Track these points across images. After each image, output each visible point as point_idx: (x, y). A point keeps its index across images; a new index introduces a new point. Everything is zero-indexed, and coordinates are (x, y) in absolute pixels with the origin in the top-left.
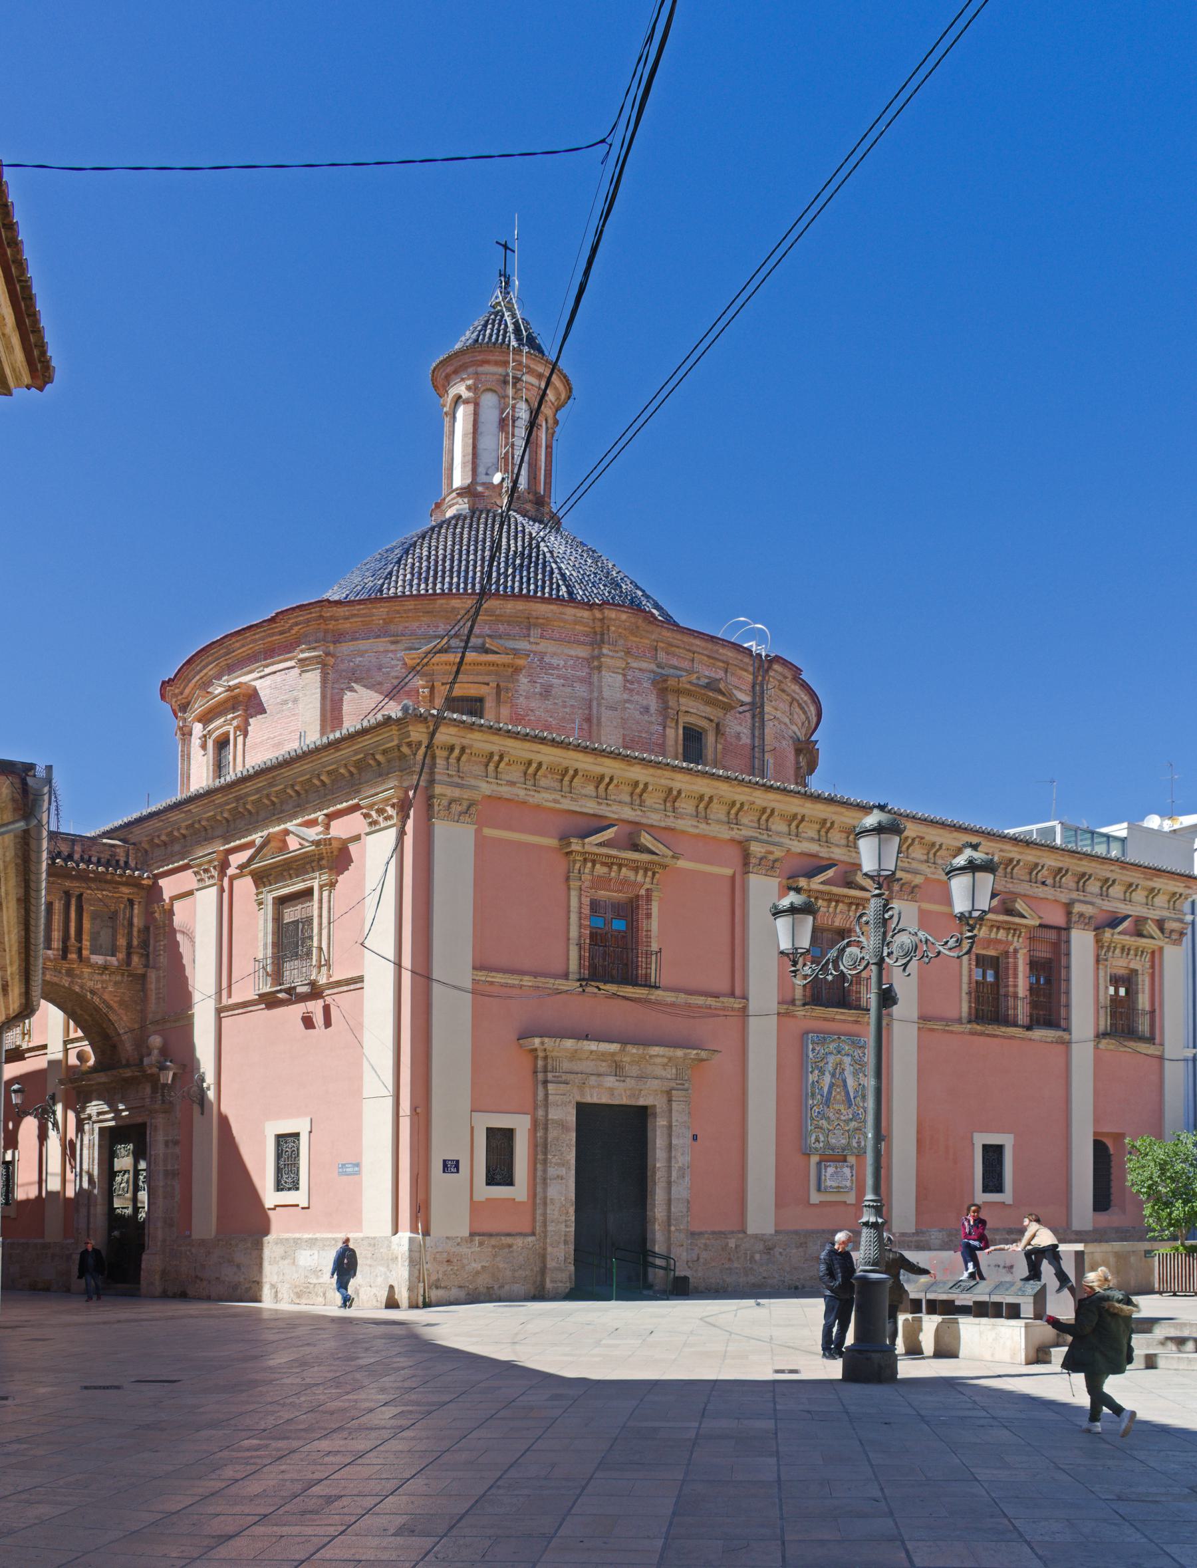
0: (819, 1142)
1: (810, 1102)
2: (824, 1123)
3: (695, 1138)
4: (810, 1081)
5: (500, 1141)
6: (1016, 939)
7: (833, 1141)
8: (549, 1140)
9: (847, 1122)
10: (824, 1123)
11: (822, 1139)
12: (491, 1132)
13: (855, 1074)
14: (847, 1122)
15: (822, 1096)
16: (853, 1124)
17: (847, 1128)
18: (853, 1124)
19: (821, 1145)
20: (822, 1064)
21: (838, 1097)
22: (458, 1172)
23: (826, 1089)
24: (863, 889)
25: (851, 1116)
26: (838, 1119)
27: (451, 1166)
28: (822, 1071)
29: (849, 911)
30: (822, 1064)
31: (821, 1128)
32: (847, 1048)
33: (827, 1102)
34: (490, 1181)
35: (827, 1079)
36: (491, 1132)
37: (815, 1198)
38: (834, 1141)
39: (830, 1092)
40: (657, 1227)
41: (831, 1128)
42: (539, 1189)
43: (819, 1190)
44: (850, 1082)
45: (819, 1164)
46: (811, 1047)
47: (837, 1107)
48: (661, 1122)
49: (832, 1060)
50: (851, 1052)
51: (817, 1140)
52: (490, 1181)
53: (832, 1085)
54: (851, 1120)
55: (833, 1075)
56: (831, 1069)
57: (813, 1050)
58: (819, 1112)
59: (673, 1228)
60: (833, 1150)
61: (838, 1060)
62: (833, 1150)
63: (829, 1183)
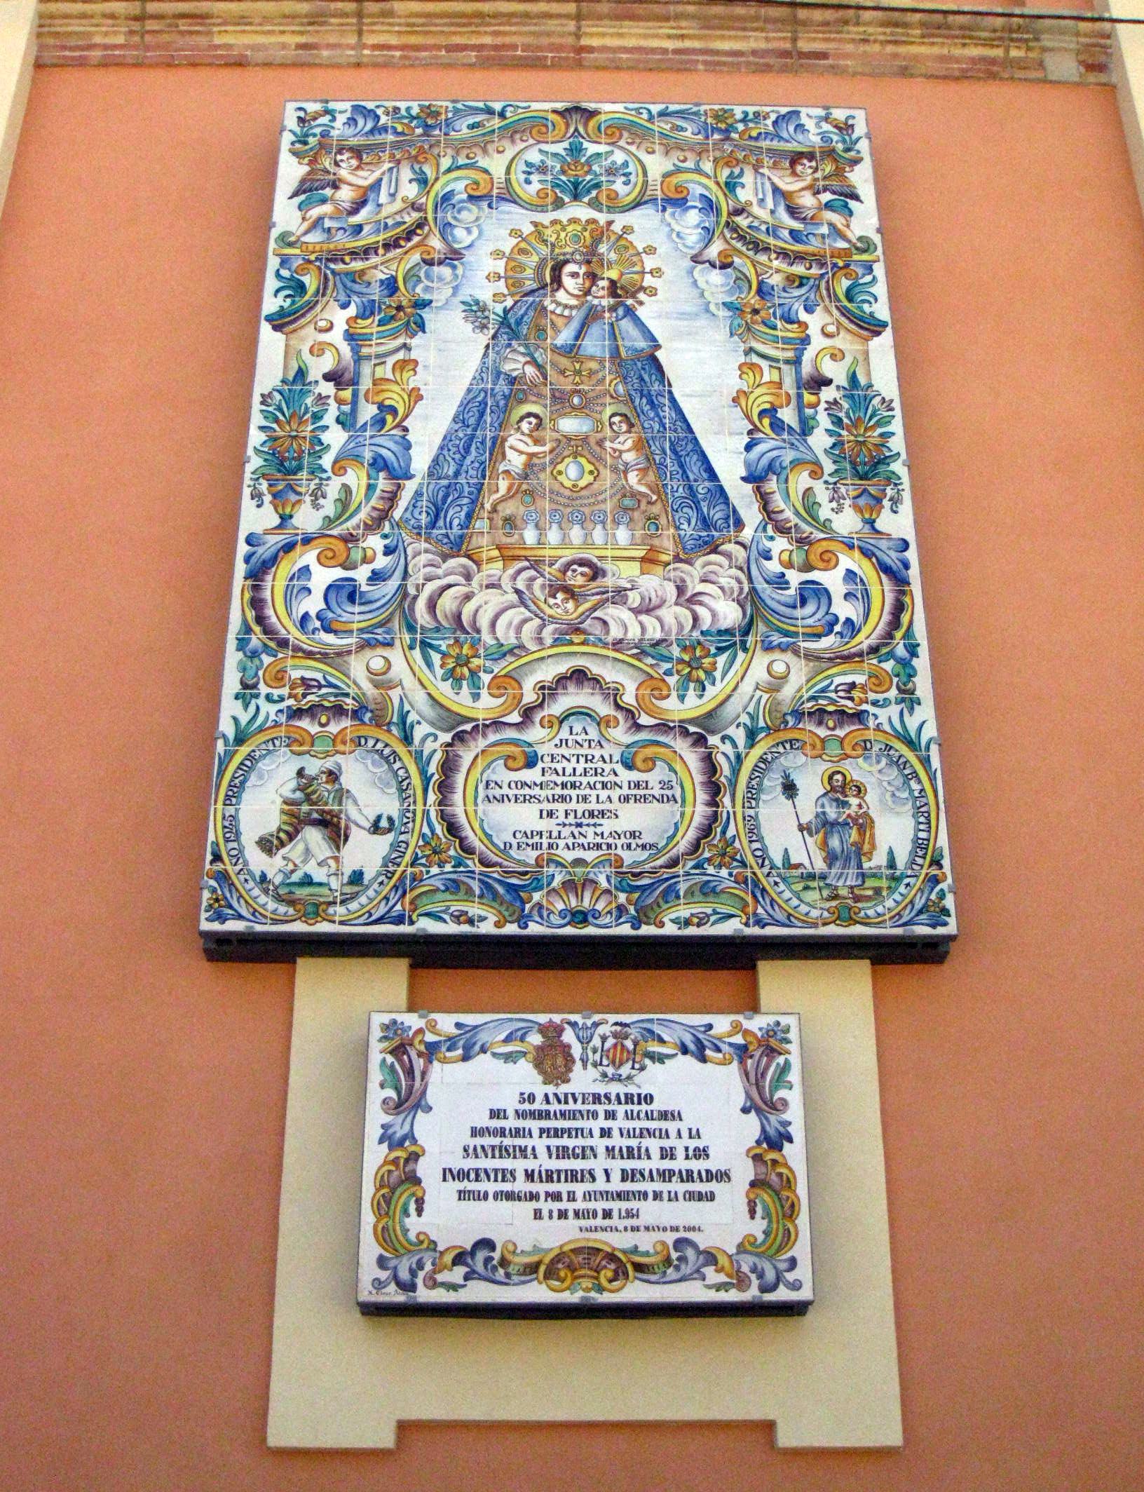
0: (335, 829)
17: (689, 706)
20: (379, 269)
21: (571, 471)
25: (730, 614)
32: (657, 165)
38: (525, 817)
41: (487, 705)
46: (290, 171)
57: (307, 189)
58: (346, 592)
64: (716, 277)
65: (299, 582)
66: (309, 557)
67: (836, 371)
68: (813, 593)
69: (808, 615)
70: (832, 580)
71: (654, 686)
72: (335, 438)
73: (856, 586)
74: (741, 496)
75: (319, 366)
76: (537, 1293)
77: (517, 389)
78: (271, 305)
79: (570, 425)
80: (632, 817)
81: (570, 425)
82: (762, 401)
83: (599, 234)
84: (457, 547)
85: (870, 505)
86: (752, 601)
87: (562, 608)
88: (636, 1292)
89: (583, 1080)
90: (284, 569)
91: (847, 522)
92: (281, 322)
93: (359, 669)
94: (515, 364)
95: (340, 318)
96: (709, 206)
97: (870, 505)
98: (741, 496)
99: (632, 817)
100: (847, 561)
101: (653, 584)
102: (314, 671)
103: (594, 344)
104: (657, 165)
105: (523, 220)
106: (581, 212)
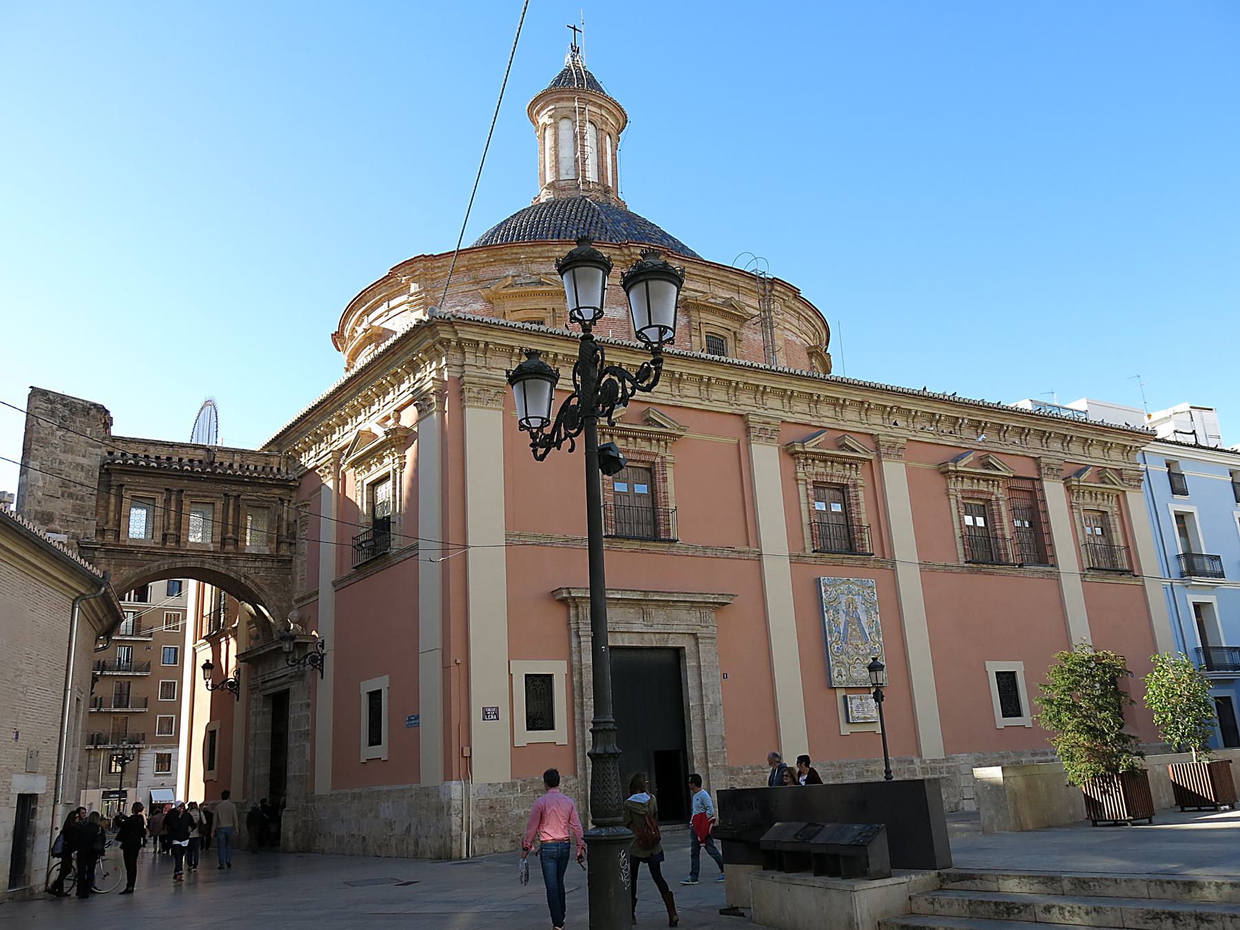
1: (829, 639)
3: (725, 676)
5: (539, 687)
6: (996, 488)
8: (584, 685)
11: (844, 673)
13: (867, 611)
21: (854, 633)
22: (498, 719)
23: (842, 627)
24: (854, 450)
26: (857, 653)
27: (490, 714)
29: (844, 470)
31: (843, 663)
32: (857, 589)
33: (845, 639)
34: (531, 726)
37: (846, 730)
39: (846, 629)
40: (695, 764)
42: (578, 732)
43: (848, 722)
45: (845, 698)
46: (823, 588)
48: (690, 663)
49: (843, 599)
52: (531, 726)
55: (847, 614)
58: (837, 648)
59: (710, 765)
63: (855, 714)
64: (863, 606)
65: (834, 648)
66: (834, 644)
67: (875, 619)
70: (876, 646)
71: (864, 659)
72: (834, 628)
73: (879, 648)
74: (868, 636)
75: (831, 619)
76: (862, 721)
77: (849, 622)
78: (825, 609)
79: (853, 627)
80: (864, 674)
81: (853, 627)
82: (869, 624)
86: (870, 649)
88: (869, 721)
89: (863, 701)
90: (832, 646)
91: (877, 639)
93: (841, 657)
94: (848, 619)
95: (832, 611)
96: (862, 595)
98: (868, 636)
99: (864, 674)
101: (862, 647)
104: (857, 589)
105: (846, 597)
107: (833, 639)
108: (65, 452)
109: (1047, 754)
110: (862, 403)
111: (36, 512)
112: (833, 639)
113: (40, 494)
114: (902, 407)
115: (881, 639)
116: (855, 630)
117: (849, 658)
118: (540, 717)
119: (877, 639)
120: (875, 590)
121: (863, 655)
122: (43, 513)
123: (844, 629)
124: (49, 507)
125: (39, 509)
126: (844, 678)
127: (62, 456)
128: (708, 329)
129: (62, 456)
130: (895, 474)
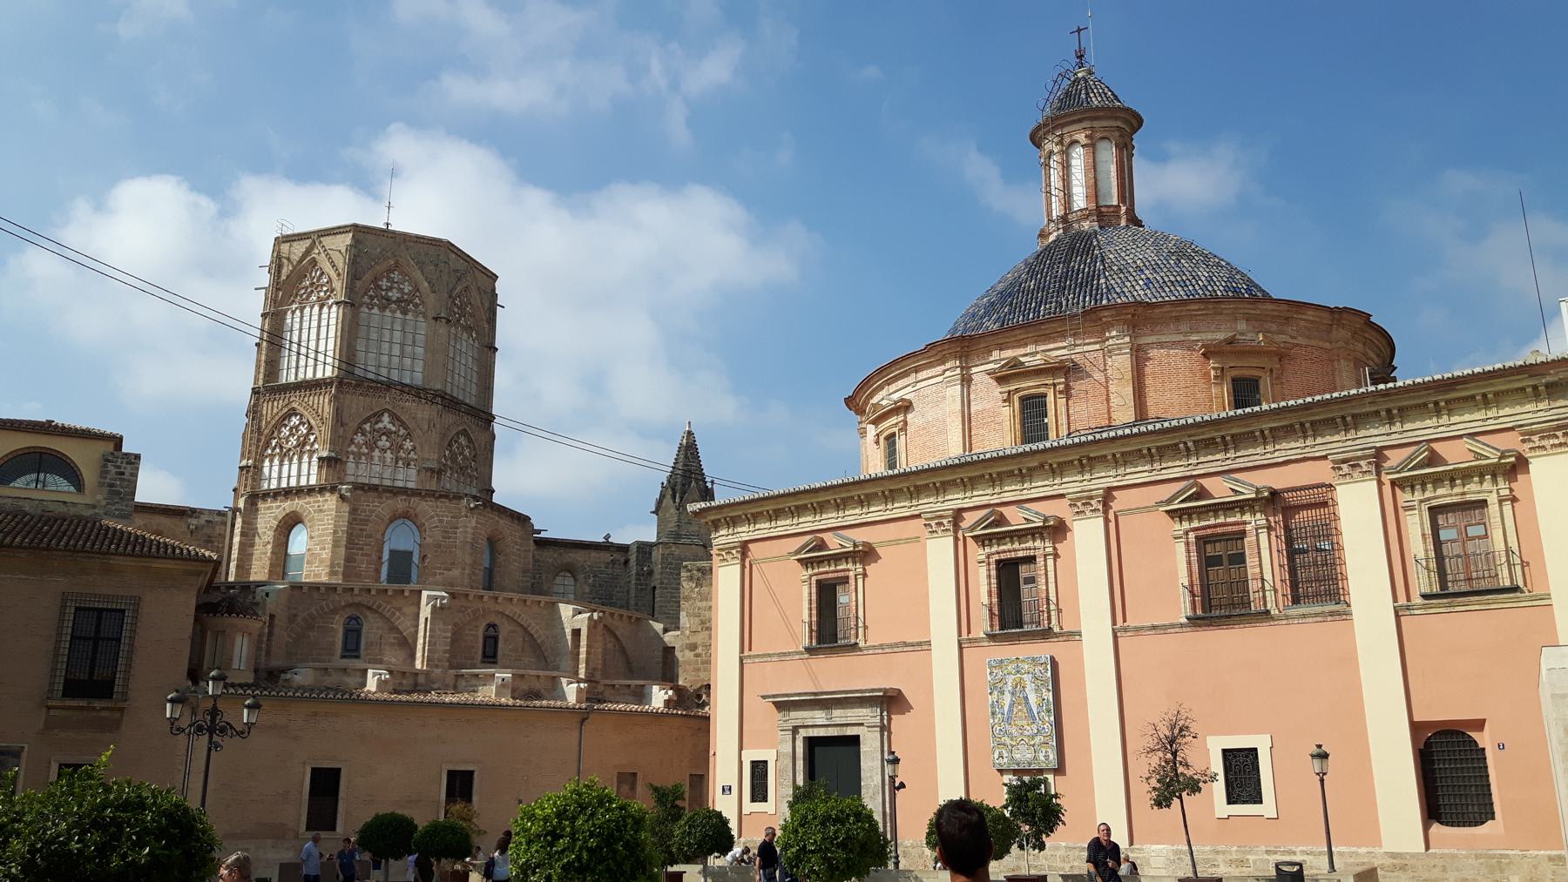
0: (1002, 757)
2: (1008, 741)
4: (990, 702)
5: (759, 769)
7: (1017, 756)
9: (1033, 737)
10: (1008, 741)
12: (755, 764)
13: (1037, 690)
14: (1033, 737)
15: (1003, 714)
16: (1038, 740)
17: (1032, 743)
18: (1038, 740)
19: (1005, 760)
20: (999, 685)
23: (1006, 708)
28: (1002, 693)
30: (999, 685)
31: (1004, 744)
32: (1026, 667)
33: (1009, 720)
35: (1007, 699)
36: (755, 764)
39: (1010, 711)
44: (1033, 699)
47: (1019, 723)
49: (1010, 680)
50: (1031, 670)
51: (1001, 756)
53: (1012, 705)
54: (1036, 735)
56: (1010, 688)
60: (1018, 764)
61: (1018, 680)
62: (1018, 764)
68: (1044, 728)
69: (1043, 731)
70: (1045, 726)
74: (1036, 715)
79: (1020, 707)
80: (1028, 756)
81: (1020, 707)
83: (1021, 679)
84: (1010, 724)
85: (1049, 716)
87: (1020, 731)
91: (1047, 719)
92: (991, 694)
97: (1049, 716)
98: (1036, 715)
99: (1028, 756)
100: (1047, 724)
101: (1028, 728)
102: (998, 740)
103: (1021, 696)
104: (1026, 667)
105: (1013, 677)
106: (1018, 675)
107: (996, 721)
108: (701, 601)
109: (1294, 853)
110: (1042, 466)
111: (687, 644)
112: (996, 721)
113: (688, 632)
114: (1091, 455)
115: (1052, 718)
116: (1020, 710)
117: (1012, 740)
118: (759, 794)
119: (1047, 719)
120: (1049, 667)
121: (1029, 736)
122: (690, 644)
123: (1009, 711)
124: (693, 640)
125: (688, 642)
126: (1005, 760)
127: (699, 604)
128: (1022, 393)
129: (699, 604)
130: (1087, 534)
